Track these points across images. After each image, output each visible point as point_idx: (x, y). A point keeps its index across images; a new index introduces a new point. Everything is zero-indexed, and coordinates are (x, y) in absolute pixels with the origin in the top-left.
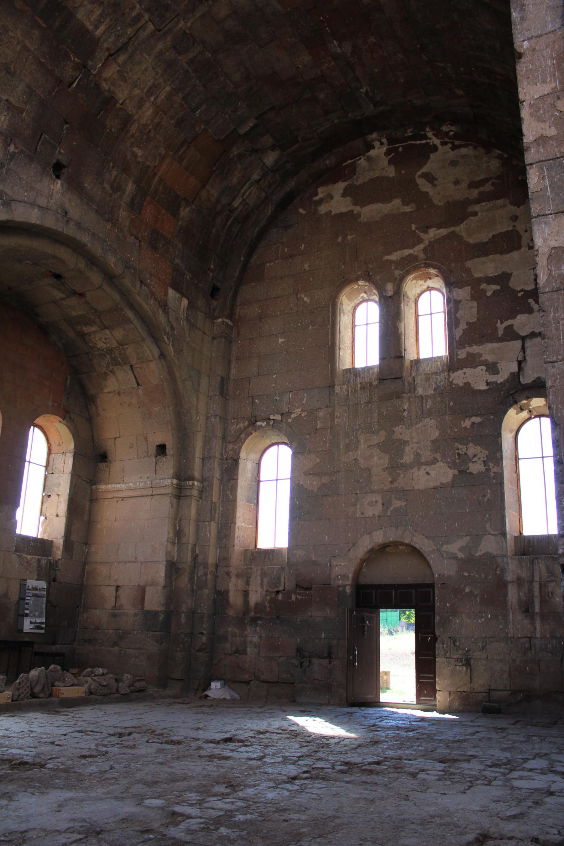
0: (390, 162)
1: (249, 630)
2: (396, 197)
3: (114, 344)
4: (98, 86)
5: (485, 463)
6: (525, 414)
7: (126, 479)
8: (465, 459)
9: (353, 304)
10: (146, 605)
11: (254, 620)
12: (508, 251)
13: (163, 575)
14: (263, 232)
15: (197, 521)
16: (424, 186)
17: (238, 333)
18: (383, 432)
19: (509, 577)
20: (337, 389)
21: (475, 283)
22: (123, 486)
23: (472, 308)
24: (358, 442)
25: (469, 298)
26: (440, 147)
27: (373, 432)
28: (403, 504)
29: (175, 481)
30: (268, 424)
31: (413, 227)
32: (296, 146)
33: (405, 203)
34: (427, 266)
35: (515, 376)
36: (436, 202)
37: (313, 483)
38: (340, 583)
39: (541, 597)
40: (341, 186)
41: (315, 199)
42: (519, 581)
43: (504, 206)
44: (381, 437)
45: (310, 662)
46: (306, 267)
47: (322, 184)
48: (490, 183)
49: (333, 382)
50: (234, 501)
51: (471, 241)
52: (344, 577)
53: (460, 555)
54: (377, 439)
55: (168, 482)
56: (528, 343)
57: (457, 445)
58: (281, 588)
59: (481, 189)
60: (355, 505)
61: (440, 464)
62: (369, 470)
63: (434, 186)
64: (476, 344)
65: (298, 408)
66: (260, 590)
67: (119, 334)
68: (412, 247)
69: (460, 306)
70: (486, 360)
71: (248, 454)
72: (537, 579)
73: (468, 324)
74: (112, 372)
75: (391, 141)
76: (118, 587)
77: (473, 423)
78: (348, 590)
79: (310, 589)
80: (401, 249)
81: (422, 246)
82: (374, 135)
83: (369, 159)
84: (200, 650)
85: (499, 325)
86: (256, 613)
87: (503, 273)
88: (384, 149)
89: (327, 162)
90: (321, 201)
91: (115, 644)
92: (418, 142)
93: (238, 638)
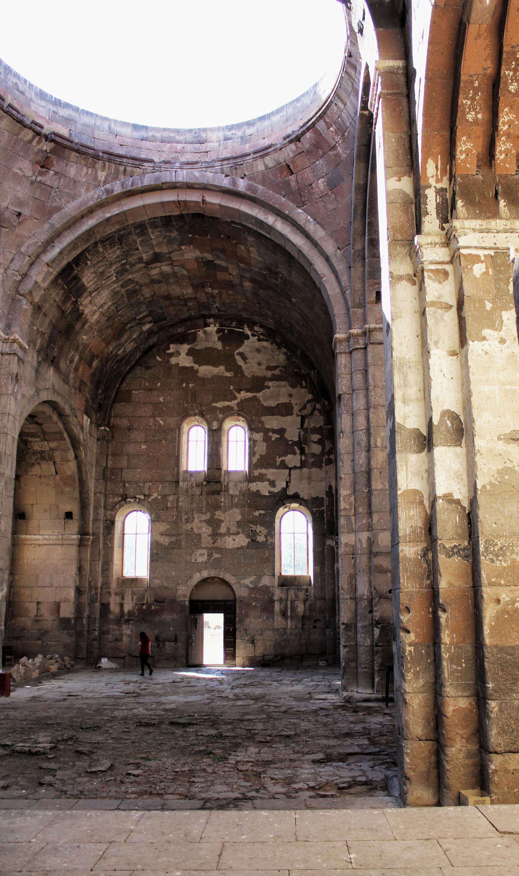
0: (219, 339)
1: (124, 627)
2: (222, 365)
3: (47, 448)
4: (78, 309)
5: (266, 536)
6: (287, 509)
7: (41, 532)
8: (255, 533)
9: (189, 427)
10: (61, 613)
11: (127, 621)
12: (286, 415)
13: (73, 595)
14: (133, 368)
15: (91, 560)
16: (240, 362)
17: (113, 437)
18: (209, 514)
19: (276, 598)
20: (181, 484)
21: (266, 431)
22: (40, 537)
23: (263, 446)
24: (193, 518)
25: (262, 440)
26: (251, 337)
27: (202, 513)
28: (220, 556)
29: (79, 536)
30: (135, 500)
31: (232, 388)
32: (164, 322)
33: (227, 370)
34: (239, 415)
35: (284, 490)
36: (246, 374)
37: (165, 541)
38: (182, 599)
39: (291, 608)
40: (185, 347)
41: (168, 352)
42: (281, 600)
43: (284, 386)
44: (208, 516)
45: (163, 644)
46: (161, 399)
47: (173, 342)
48: (279, 369)
49: (178, 479)
50: (112, 548)
51: (265, 404)
52: (185, 596)
53: (251, 586)
54: (204, 517)
55: (75, 537)
56: (292, 472)
57: (251, 525)
58: (145, 602)
59: (273, 372)
60: (191, 555)
61: (241, 535)
62: (200, 535)
63: (246, 363)
64: (264, 468)
65: (155, 492)
66: (131, 602)
67: (53, 444)
68: (231, 401)
69: (256, 444)
70: (269, 479)
71: (119, 517)
72: (289, 599)
73: (260, 455)
74: (39, 464)
75: (221, 325)
76: (38, 602)
77: (260, 514)
78: (187, 603)
79: (164, 602)
80: (224, 401)
81: (236, 402)
82: (211, 320)
83: (205, 332)
84: (93, 640)
85: (277, 459)
86: (129, 616)
87: (282, 428)
88: (216, 328)
89: (179, 330)
90: (171, 355)
91: (39, 639)
92: (237, 330)
93: (117, 632)
